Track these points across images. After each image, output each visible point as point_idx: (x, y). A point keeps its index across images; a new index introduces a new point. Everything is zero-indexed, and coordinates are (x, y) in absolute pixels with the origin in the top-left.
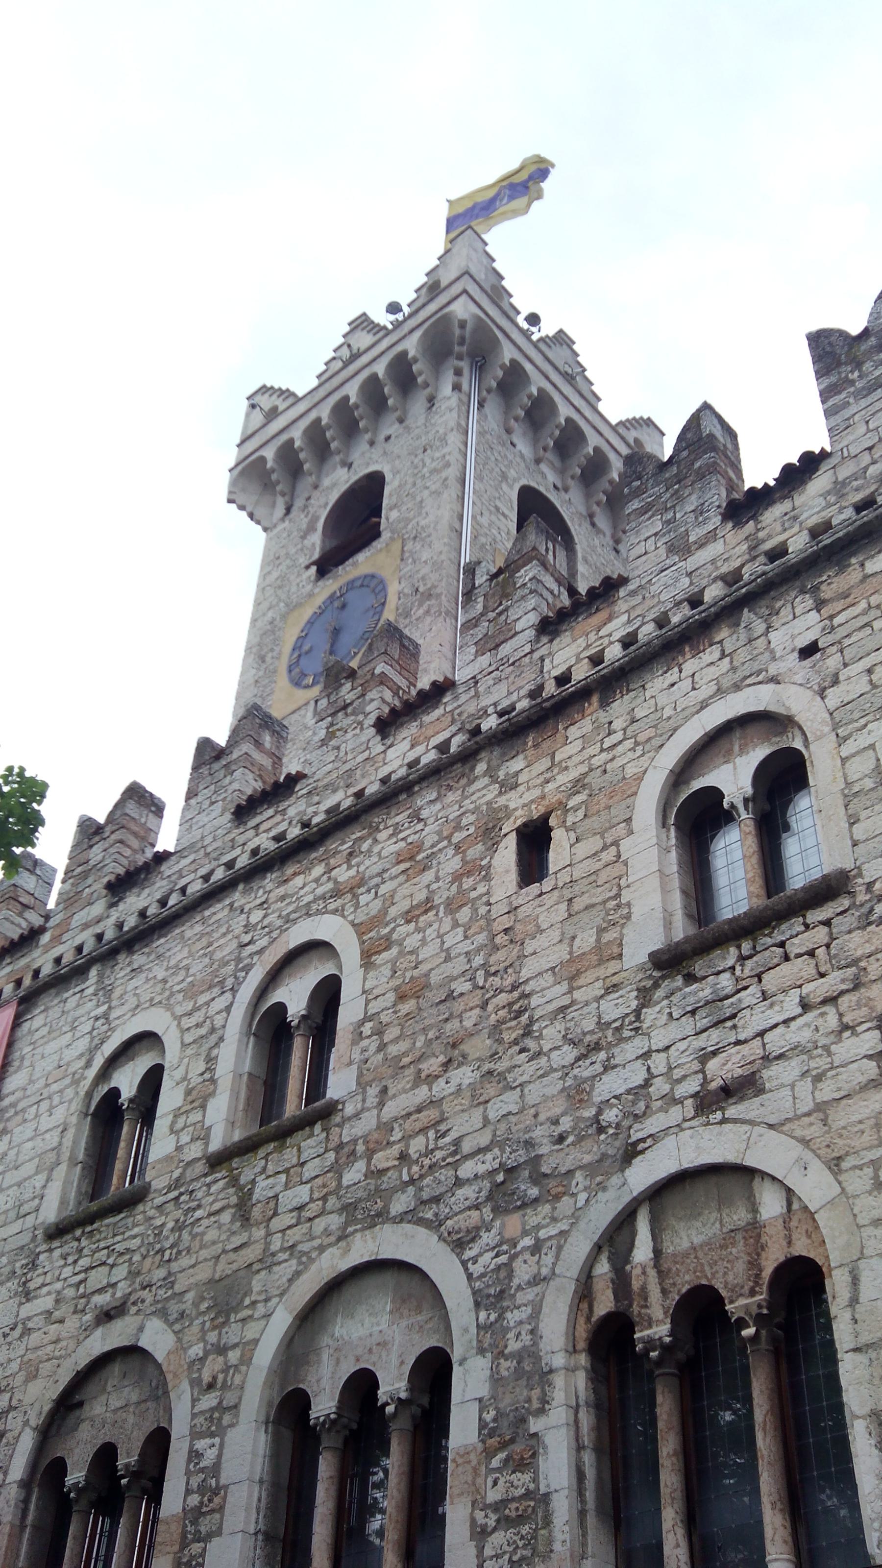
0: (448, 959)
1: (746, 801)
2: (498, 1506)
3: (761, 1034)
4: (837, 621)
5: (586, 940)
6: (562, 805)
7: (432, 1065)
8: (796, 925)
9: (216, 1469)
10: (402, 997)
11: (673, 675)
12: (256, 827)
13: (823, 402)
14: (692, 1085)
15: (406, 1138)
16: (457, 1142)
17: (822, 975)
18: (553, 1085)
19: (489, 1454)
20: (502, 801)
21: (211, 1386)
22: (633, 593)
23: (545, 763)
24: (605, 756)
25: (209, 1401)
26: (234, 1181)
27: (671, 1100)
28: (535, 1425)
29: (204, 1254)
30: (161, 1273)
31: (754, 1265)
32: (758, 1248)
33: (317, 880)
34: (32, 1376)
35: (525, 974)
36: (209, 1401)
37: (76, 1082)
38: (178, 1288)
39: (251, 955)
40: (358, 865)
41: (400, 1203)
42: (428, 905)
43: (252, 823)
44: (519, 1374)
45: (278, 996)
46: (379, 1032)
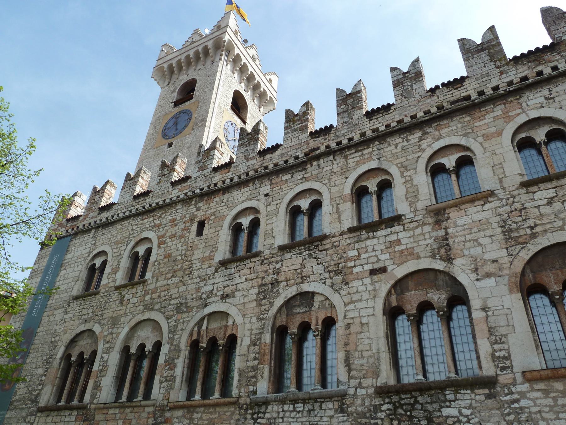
0: (177, 250)
1: (247, 228)
2: (165, 377)
3: (237, 284)
4: (274, 189)
5: (207, 254)
6: (209, 218)
7: (169, 275)
8: (248, 261)
9: (107, 361)
10: (165, 257)
11: (239, 191)
12: (138, 202)
13: (285, 130)
14: (221, 293)
15: (161, 292)
16: (171, 295)
17: (251, 274)
18: (194, 286)
19: (166, 366)
20: (196, 213)
21: (108, 342)
22: (235, 167)
23: (207, 206)
24: (220, 208)
25: (107, 345)
26: (120, 294)
27: (216, 295)
28: (176, 361)
29: (111, 310)
30: (100, 313)
31: (225, 334)
32: (226, 330)
33: (150, 222)
34: (65, 333)
35: (193, 258)
36: (107, 345)
37: (85, 260)
38: (104, 317)
39: (132, 237)
40: (161, 220)
41: (157, 306)
42: (175, 235)
43: (137, 201)
44: (175, 349)
45: (137, 249)
46: (159, 265)
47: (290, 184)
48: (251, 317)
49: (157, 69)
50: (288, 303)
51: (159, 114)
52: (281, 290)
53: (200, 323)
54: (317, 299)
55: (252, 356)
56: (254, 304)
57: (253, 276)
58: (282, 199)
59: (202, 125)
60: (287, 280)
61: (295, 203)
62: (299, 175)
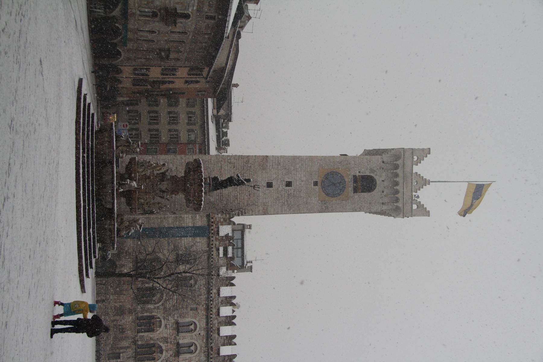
4: (201, 337)
6: (197, 312)
27: (167, 322)
47: (201, 343)
48: (158, 336)
49: (400, 152)
50: (161, 347)
51: (353, 162)
52: (164, 345)
53: (159, 318)
54: (160, 355)
55: (147, 338)
56: (162, 336)
57: (171, 334)
58: (196, 341)
59: (323, 209)
60: (167, 346)
61: (194, 344)
62: (203, 345)
